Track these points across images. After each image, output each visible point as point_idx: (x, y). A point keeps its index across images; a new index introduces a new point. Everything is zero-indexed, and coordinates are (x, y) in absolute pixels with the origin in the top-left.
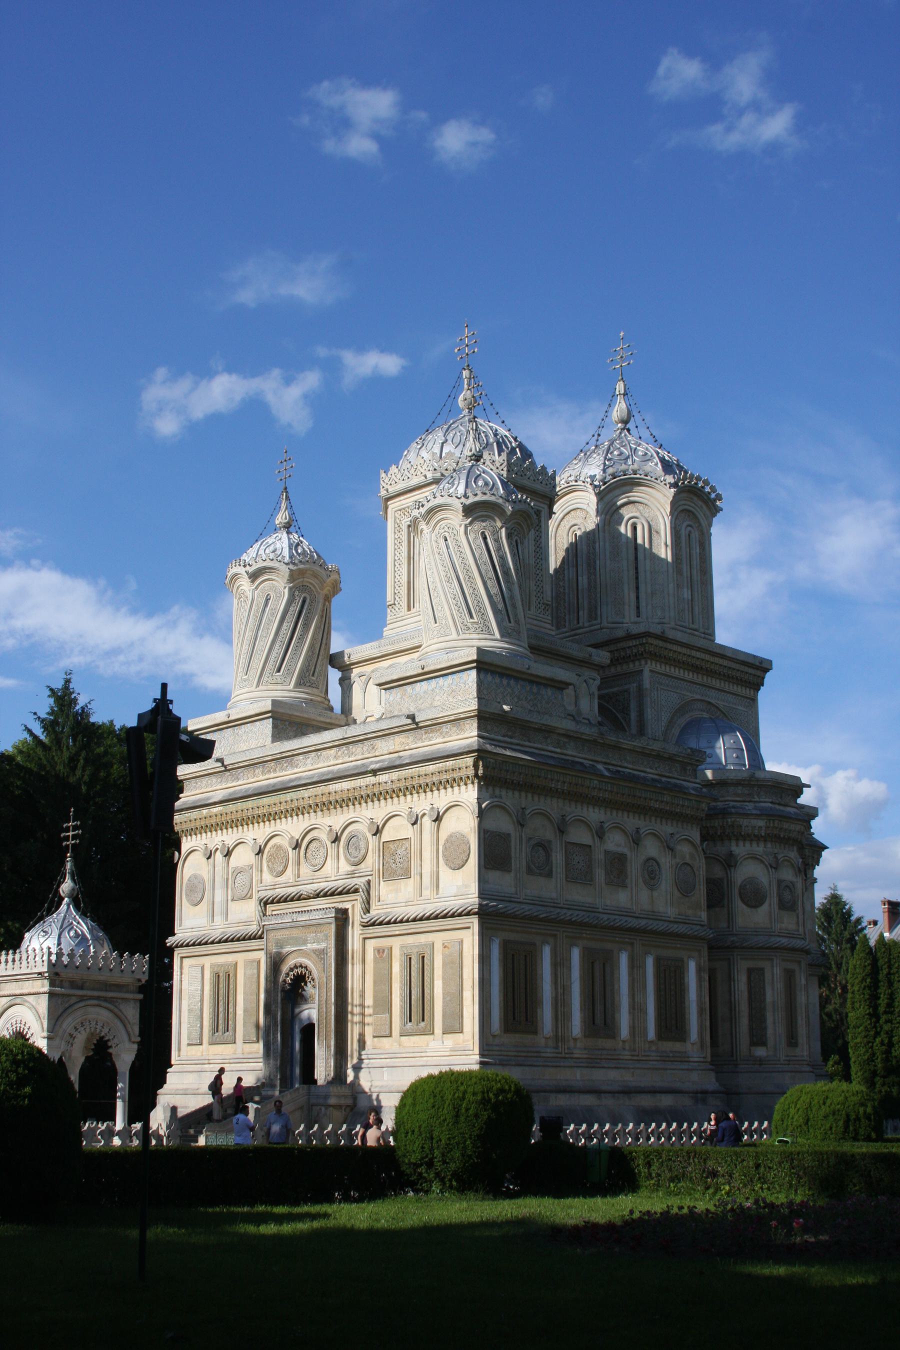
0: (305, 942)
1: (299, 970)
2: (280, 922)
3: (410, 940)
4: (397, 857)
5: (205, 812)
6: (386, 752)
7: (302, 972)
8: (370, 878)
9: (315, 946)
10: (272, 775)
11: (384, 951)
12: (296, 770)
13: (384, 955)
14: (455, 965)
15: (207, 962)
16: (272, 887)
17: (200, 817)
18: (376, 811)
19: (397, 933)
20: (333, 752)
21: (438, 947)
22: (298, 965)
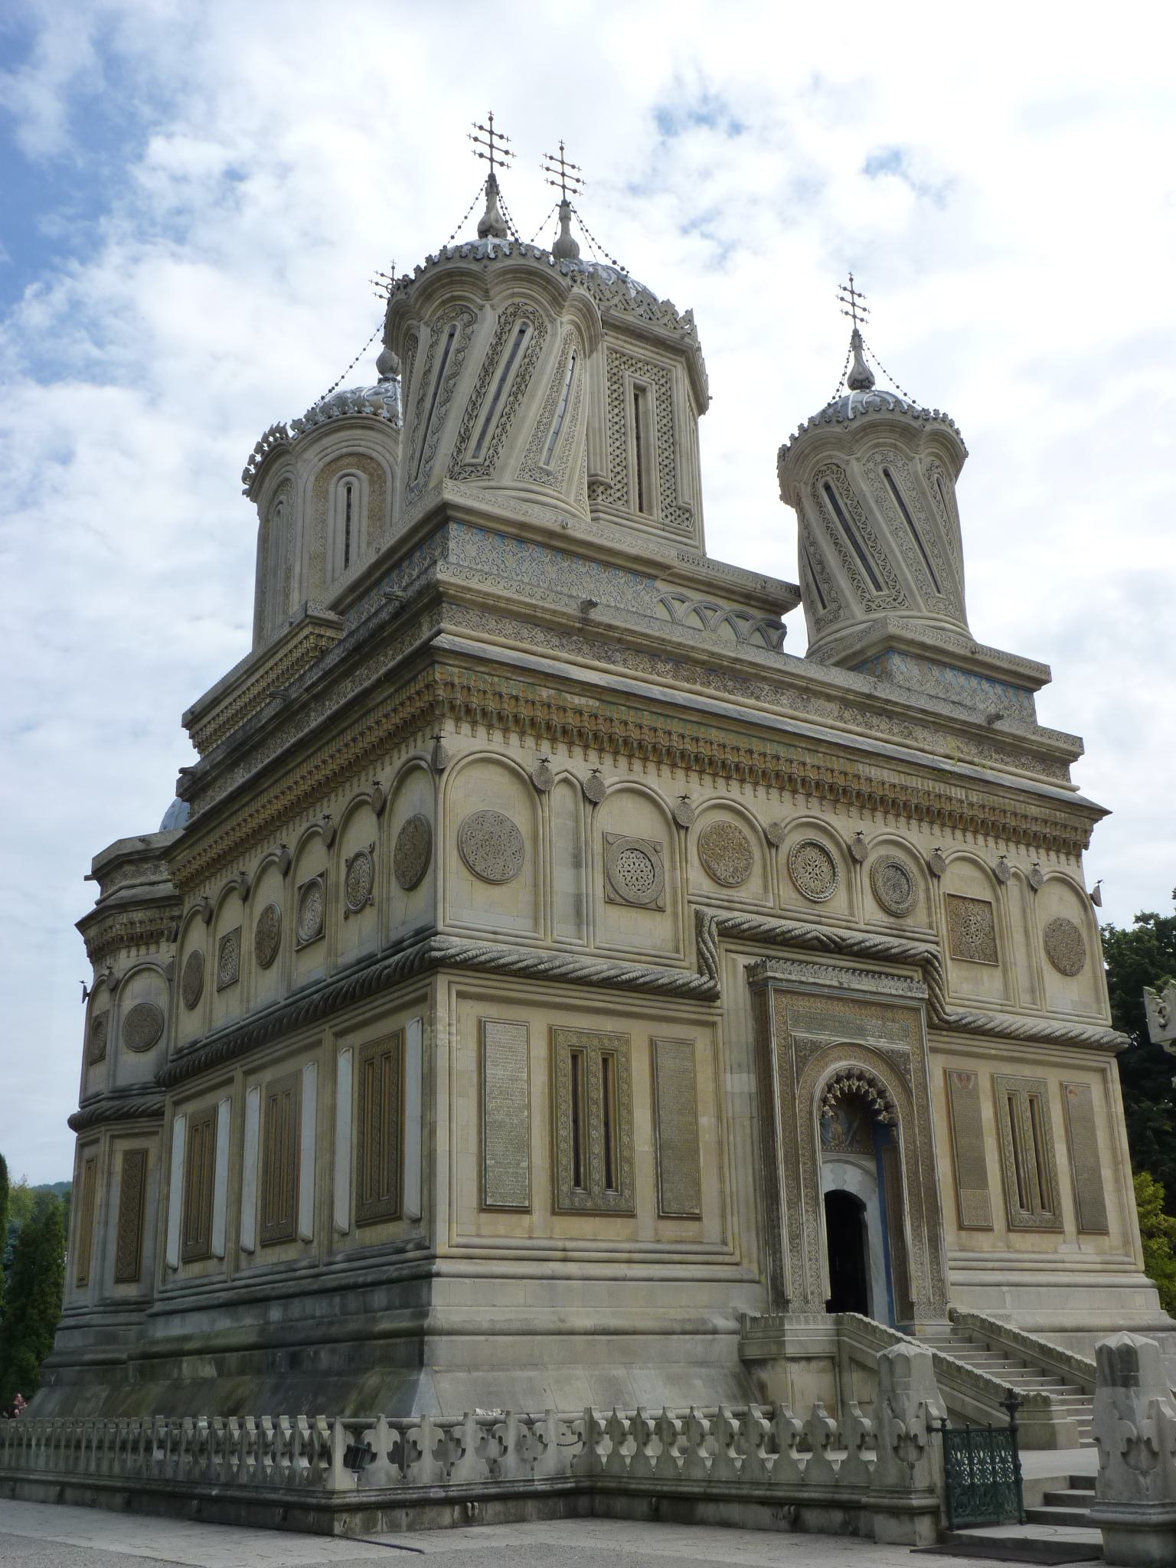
0: (861, 1032)
1: (855, 1084)
2: (812, 980)
3: (1008, 1069)
4: (973, 928)
5: (545, 693)
6: (942, 751)
7: (859, 1086)
8: (934, 946)
9: (883, 1044)
10: (698, 687)
11: (968, 1079)
12: (752, 702)
13: (958, 1085)
14: (1078, 1123)
15: (539, 1022)
16: (726, 904)
17: (530, 697)
18: (950, 843)
19: (993, 1052)
20: (833, 707)
21: (1053, 1090)
22: (856, 1072)
